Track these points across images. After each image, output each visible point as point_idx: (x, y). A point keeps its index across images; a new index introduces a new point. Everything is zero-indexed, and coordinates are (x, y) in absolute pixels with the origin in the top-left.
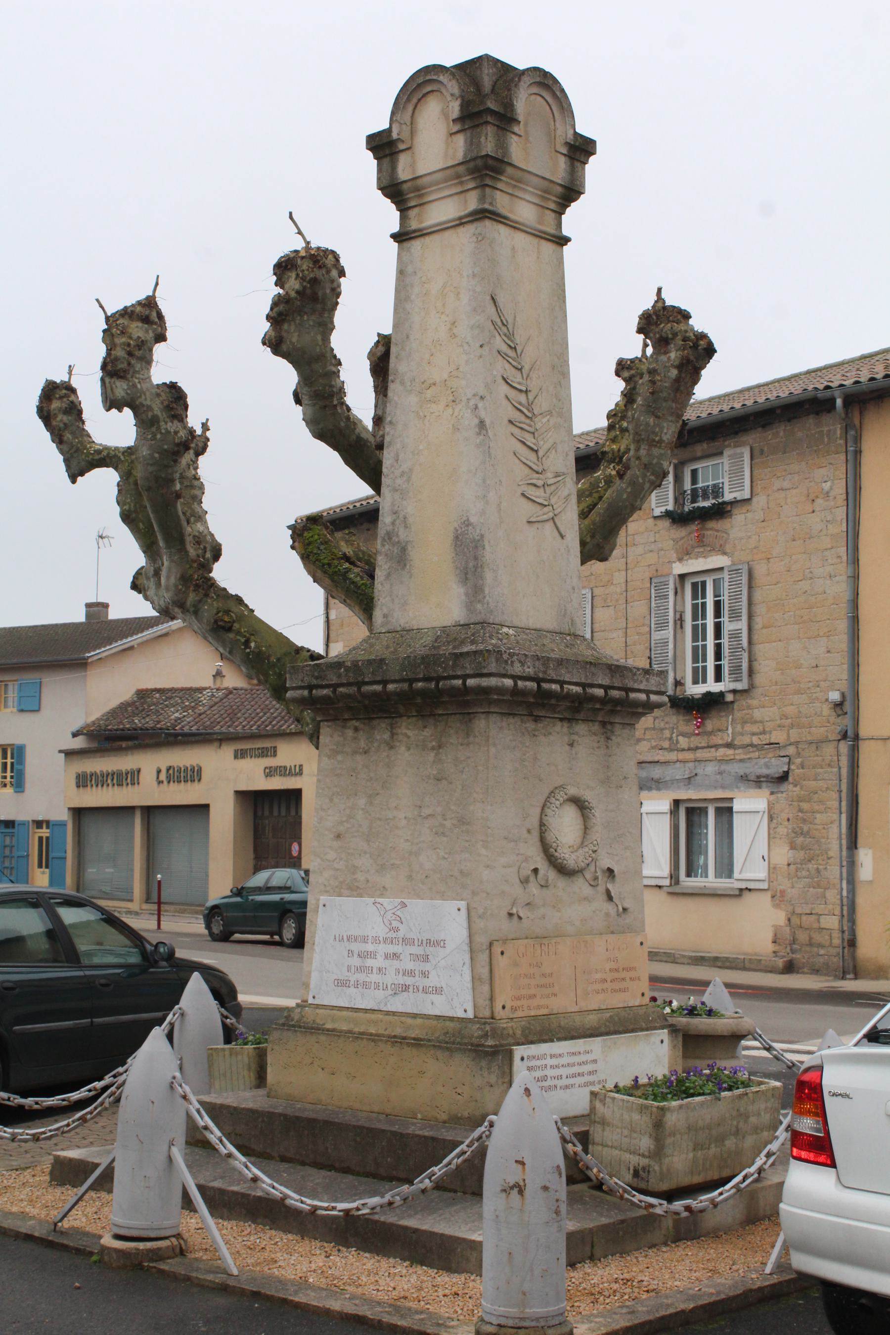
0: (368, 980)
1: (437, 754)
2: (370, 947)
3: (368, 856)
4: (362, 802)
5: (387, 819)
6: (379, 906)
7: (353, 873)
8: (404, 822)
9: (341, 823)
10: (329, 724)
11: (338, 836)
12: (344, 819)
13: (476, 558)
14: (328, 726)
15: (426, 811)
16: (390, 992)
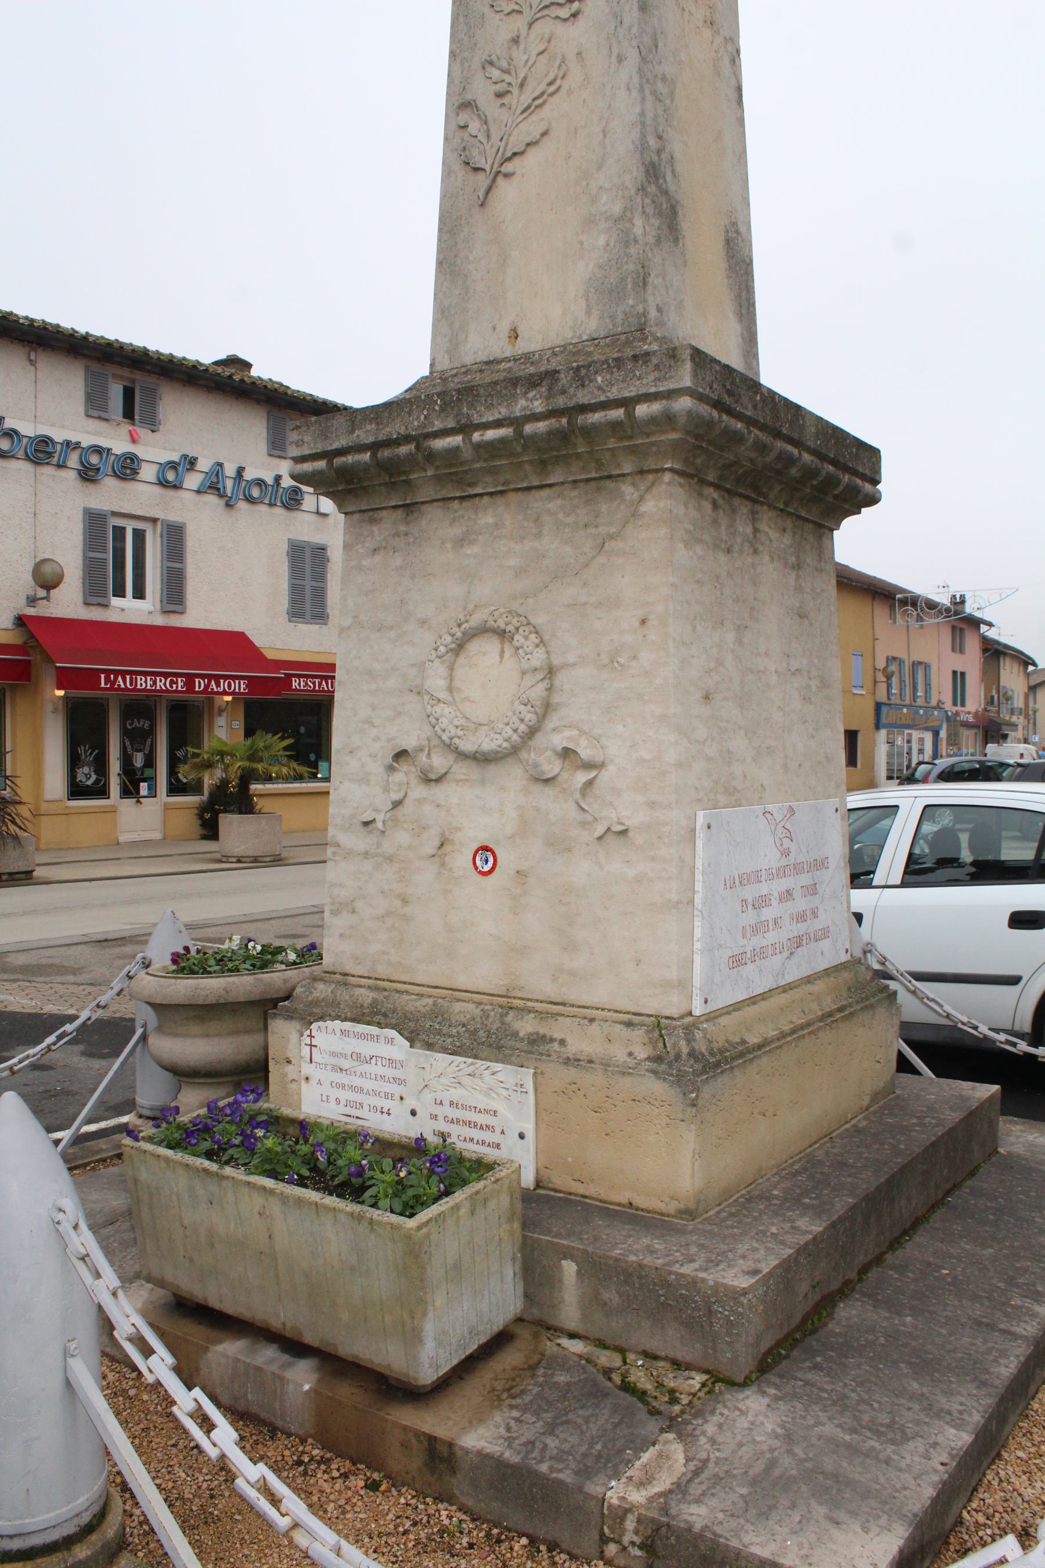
0: (764, 943)
1: (798, 577)
2: (764, 889)
3: (742, 732)
4: (730, 637)
5: (759, 672)
6: (768, 816)
7: (729, 764)
8: (774, 679)
9: (709, 672)
10: (681, 480)
11: (707, 697)
12: (712, 665)
13: (747, 285)
14: (681, 485)
15: (795, 664)
16: (787, 953)
